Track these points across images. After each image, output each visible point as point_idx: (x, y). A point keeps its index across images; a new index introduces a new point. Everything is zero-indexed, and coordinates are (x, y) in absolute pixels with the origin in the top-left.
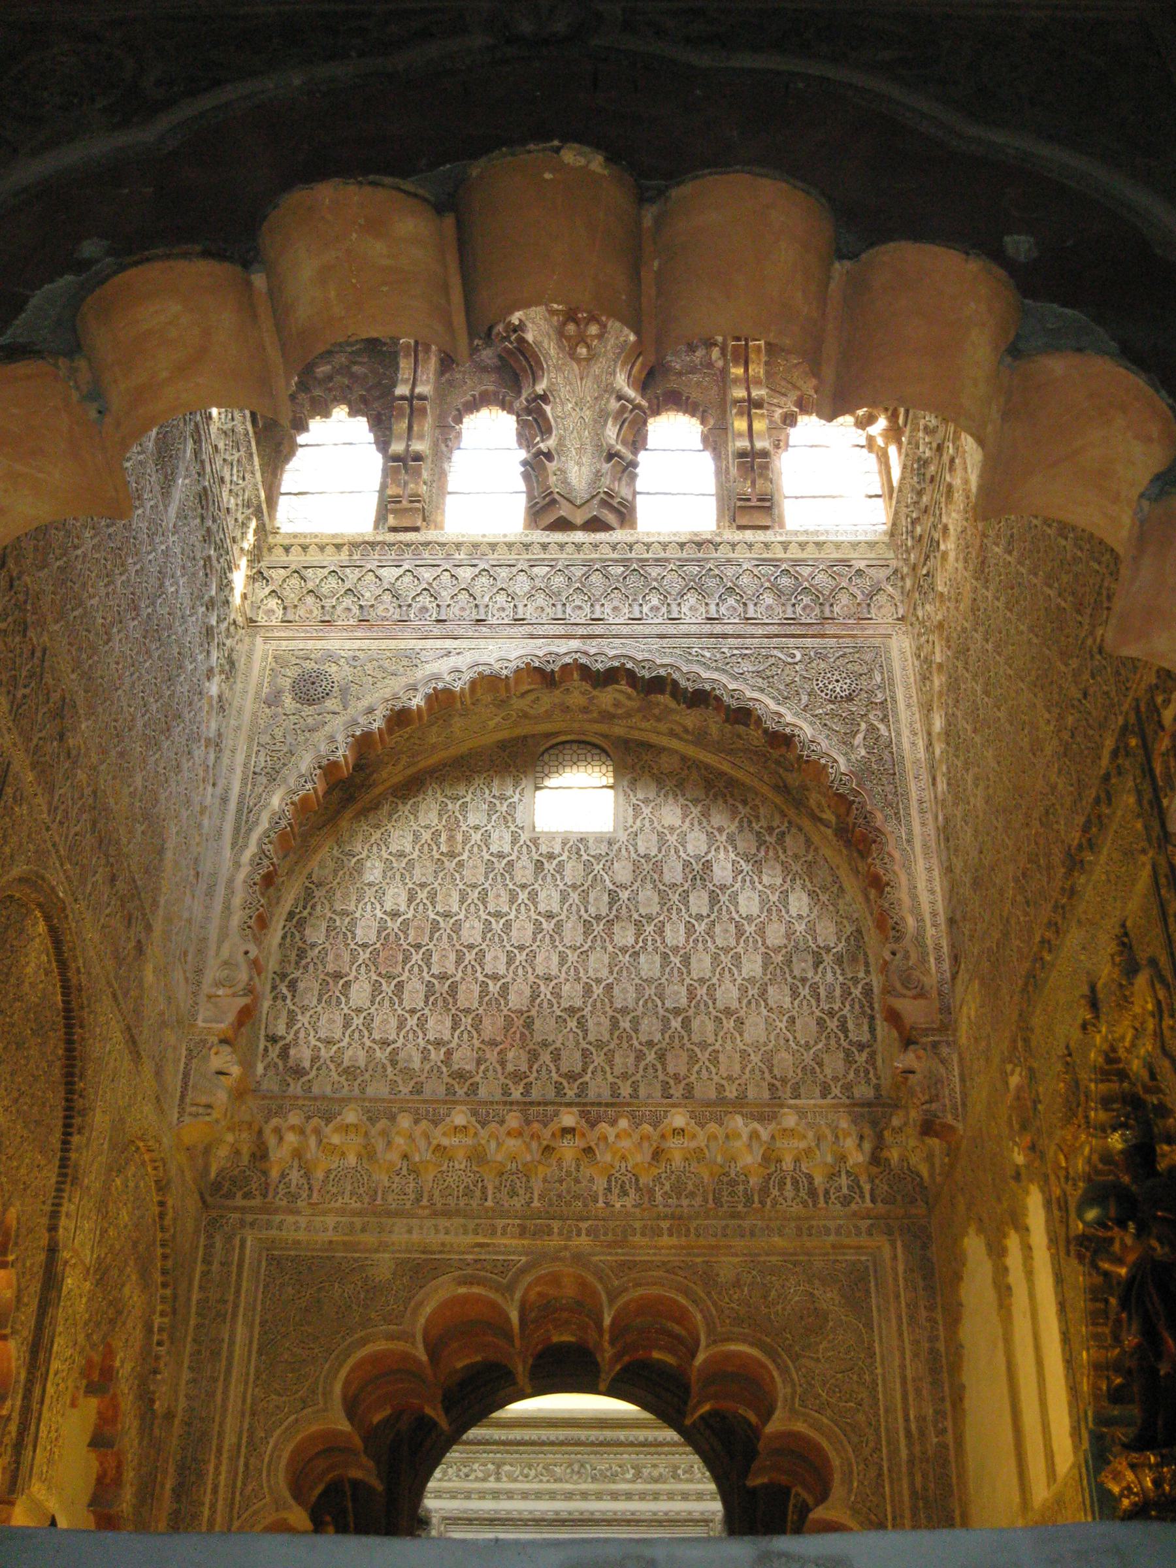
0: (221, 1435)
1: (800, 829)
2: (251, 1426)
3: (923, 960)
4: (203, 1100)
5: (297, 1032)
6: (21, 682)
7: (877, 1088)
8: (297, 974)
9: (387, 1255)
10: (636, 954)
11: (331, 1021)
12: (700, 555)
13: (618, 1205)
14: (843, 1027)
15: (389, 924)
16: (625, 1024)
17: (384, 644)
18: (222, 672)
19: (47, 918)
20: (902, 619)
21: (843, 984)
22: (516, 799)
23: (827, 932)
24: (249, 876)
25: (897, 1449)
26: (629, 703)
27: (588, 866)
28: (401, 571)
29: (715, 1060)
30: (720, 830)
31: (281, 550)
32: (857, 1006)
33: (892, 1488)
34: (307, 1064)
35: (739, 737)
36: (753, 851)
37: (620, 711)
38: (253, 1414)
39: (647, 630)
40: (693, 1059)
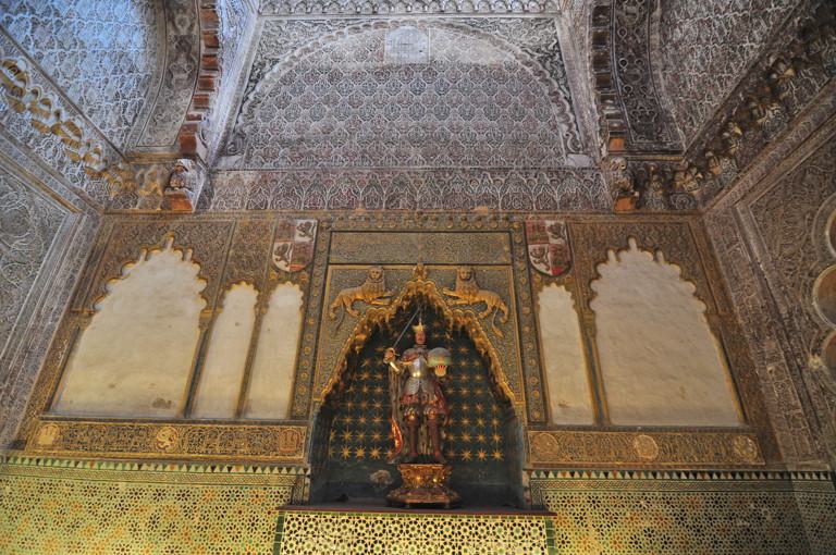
7: (123, 145)
14: (125, 106)
23: (141, 64)
33: (11, 340)
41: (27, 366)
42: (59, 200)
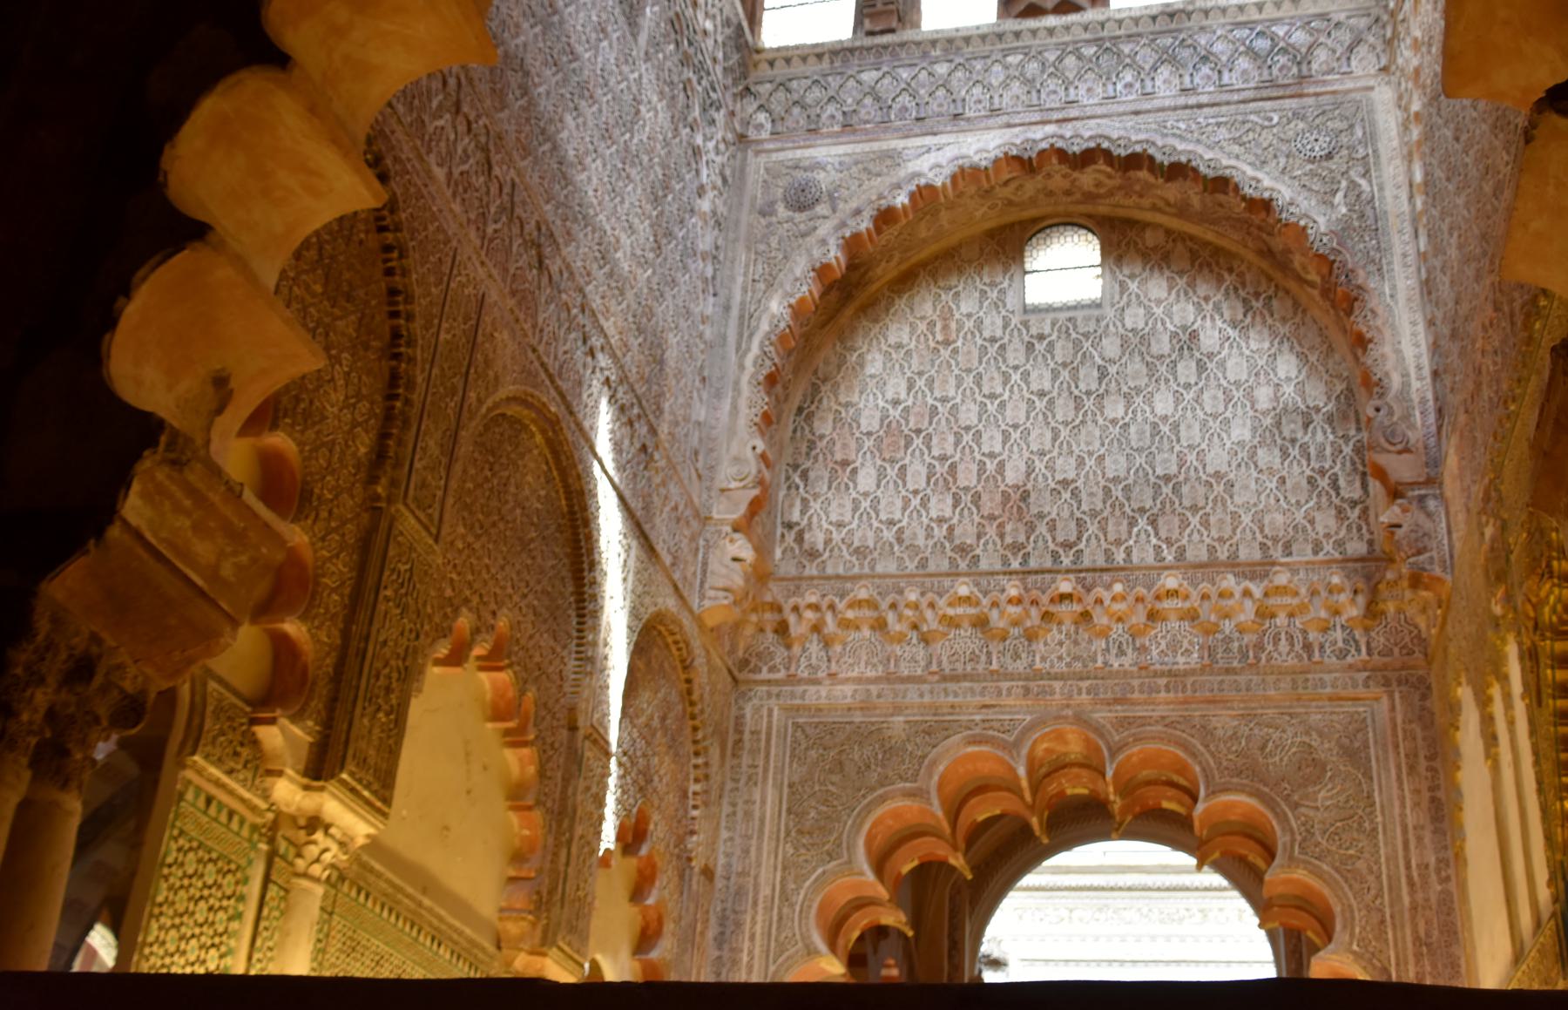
0: (756, 886)
1: (1287, 292)
2: (783, 879)
3: (1407, 417)
4: (721, 583)
5: (810, 518)
6: (490, 218)
7: (1371, 543)
8: (808, 464)
9: (901, 719)
10: (1126, 425)
11: (841, 506)
12: (1173, 26)
13: (1116, 665)
15: (891, 411)
16: (1117, 492)
17: (866, 147)
18: (714, 188)
19: (543, 432)
20: (1384, 69)
21: (1332, 443)
22: (1005, 284)
23: (1317, 395)
24: (752, 376)
25: (1400, 897)
26: (1107, 181)
27: (1077, 345)
28: (880, 74)
29: (1206, 523)
30: (1207, 299)
31: (765, 66)
32: (1348, 464)
34: (820, 547)
35: (1221, 205)
36: (1240, 316)
37: (1102, 191)
38: (784, 868)
39: (1121, 109)
40: (1184, 524)
41: (1434, 966)
42: (1341, 699)
